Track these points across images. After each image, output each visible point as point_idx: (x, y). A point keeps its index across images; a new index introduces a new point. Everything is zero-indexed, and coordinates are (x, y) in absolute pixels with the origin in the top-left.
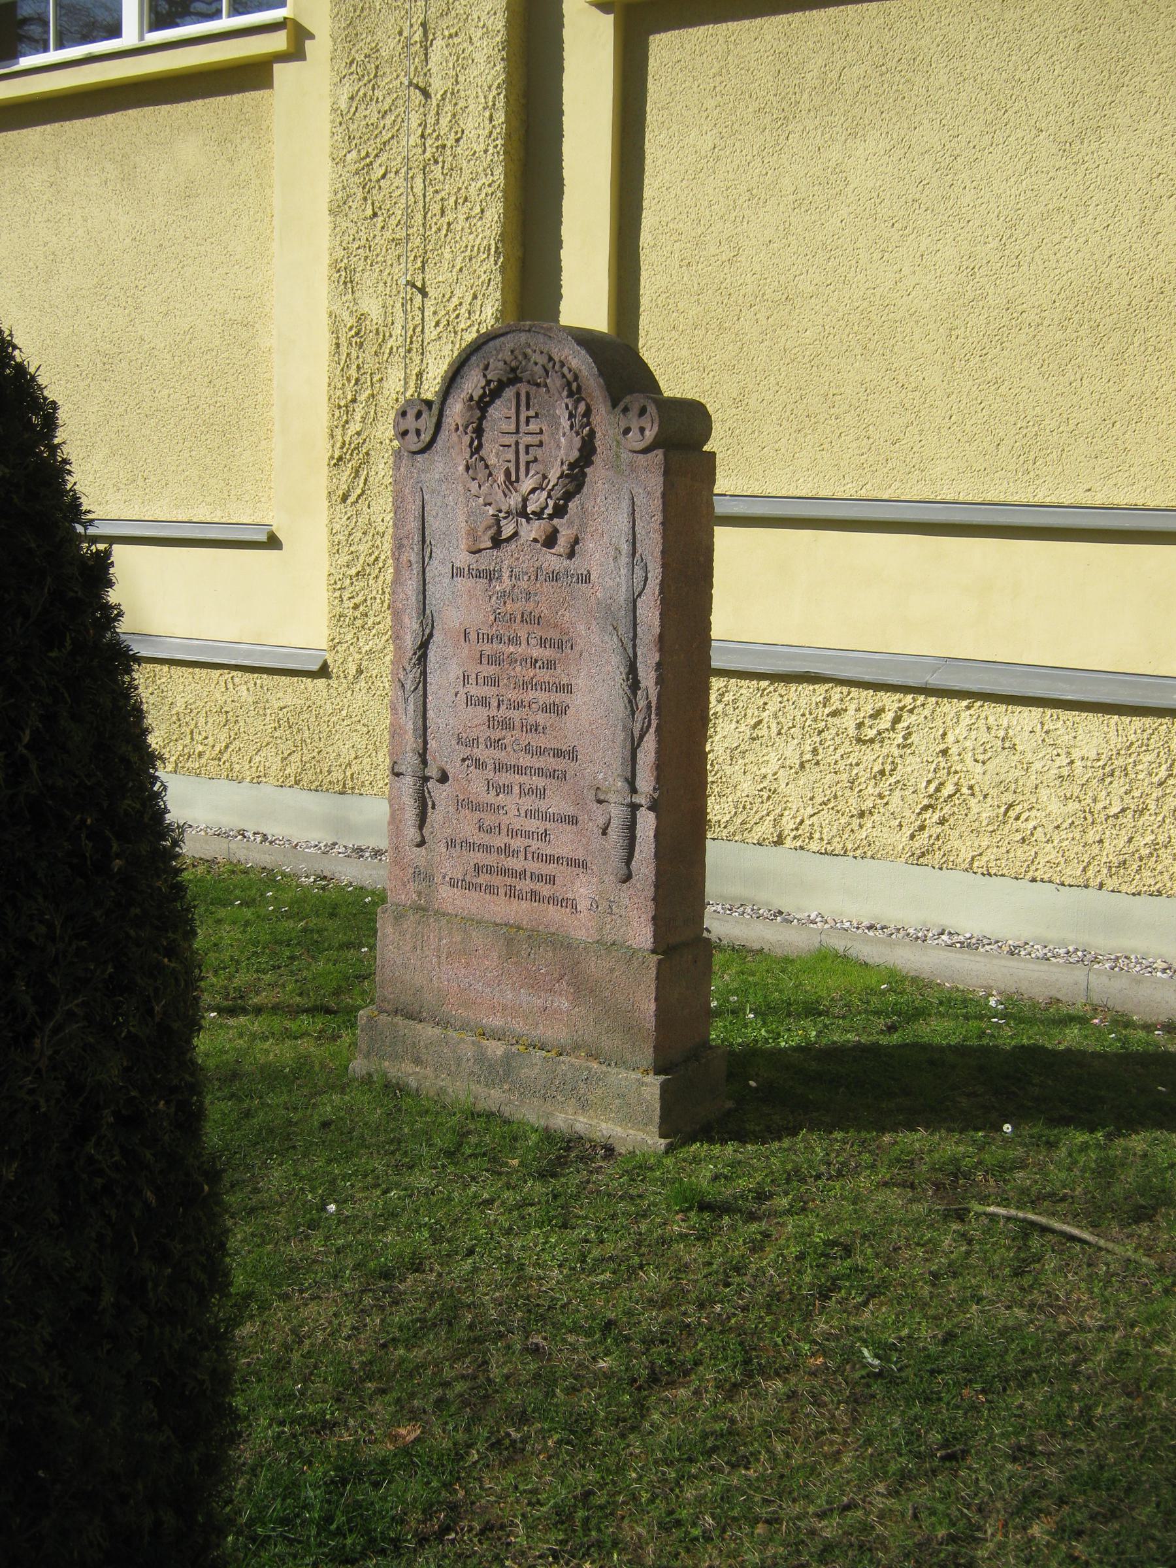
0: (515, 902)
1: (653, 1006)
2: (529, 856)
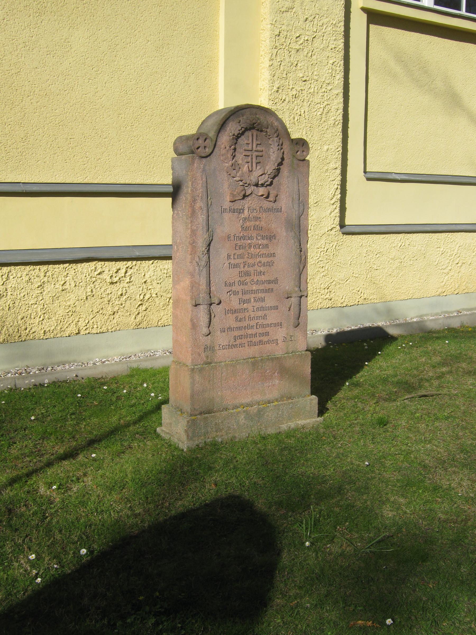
0: (252, 348)
1: (310, 370)
2: (258, 327)
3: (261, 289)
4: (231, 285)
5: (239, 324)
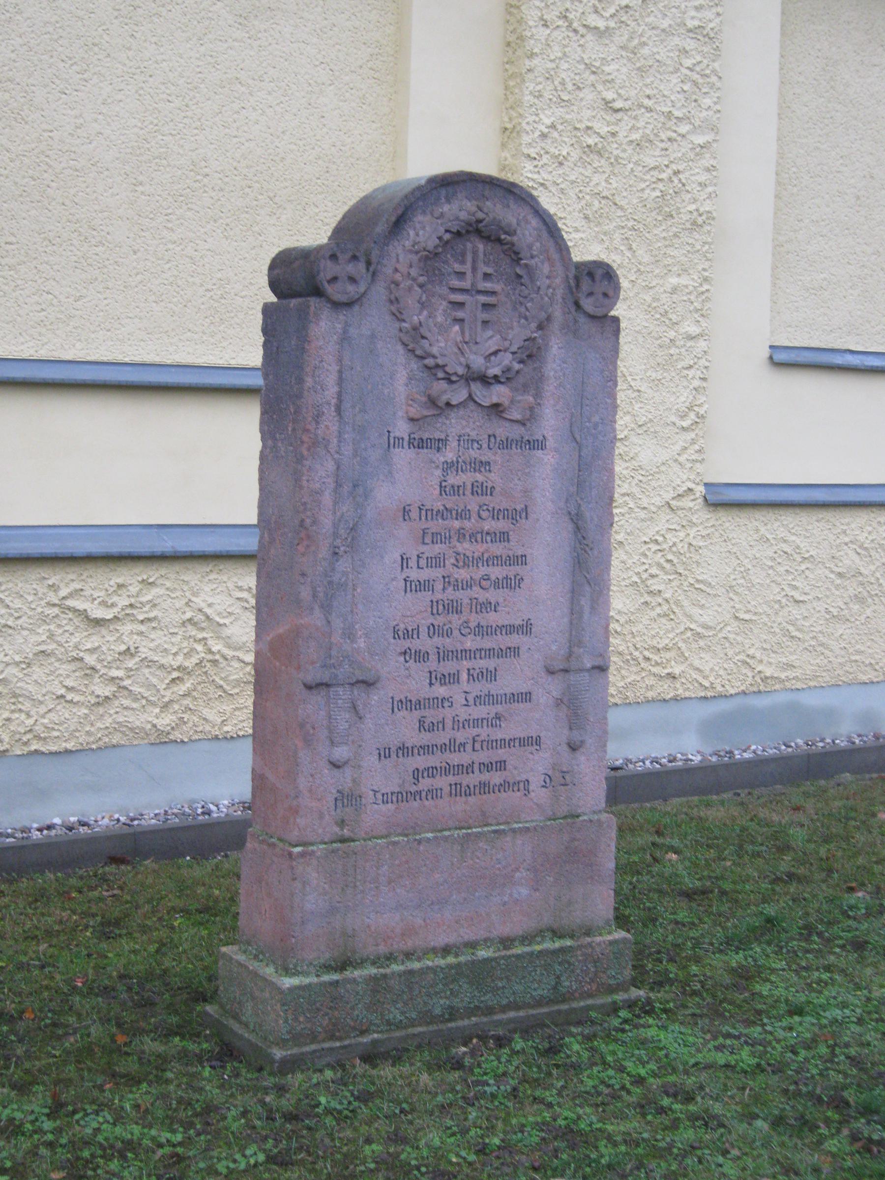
0: (461, 800)
3: (488, 648)
4: (408, 634)
5: (426, 738)
